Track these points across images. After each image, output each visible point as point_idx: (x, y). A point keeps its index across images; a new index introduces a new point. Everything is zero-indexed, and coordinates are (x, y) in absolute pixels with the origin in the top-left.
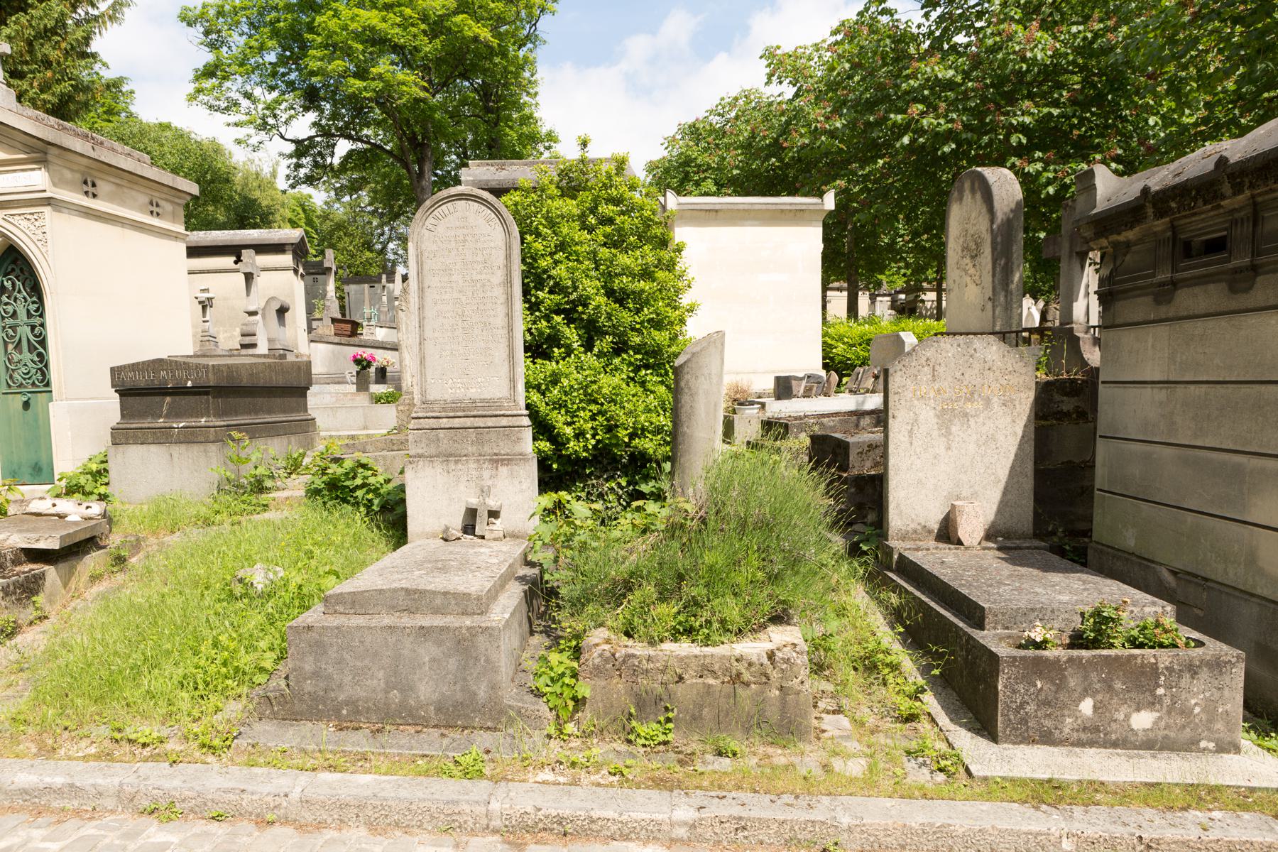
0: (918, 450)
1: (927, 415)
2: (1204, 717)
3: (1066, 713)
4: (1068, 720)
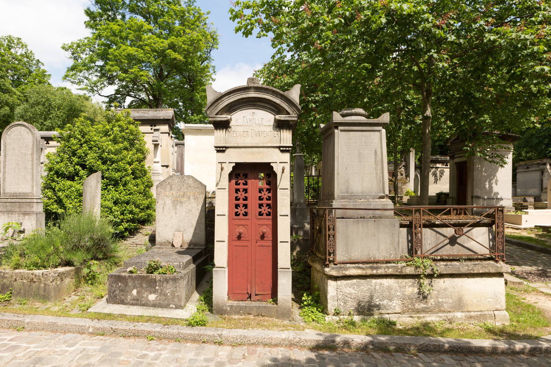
1: (169, 202)
4: (129, 296)
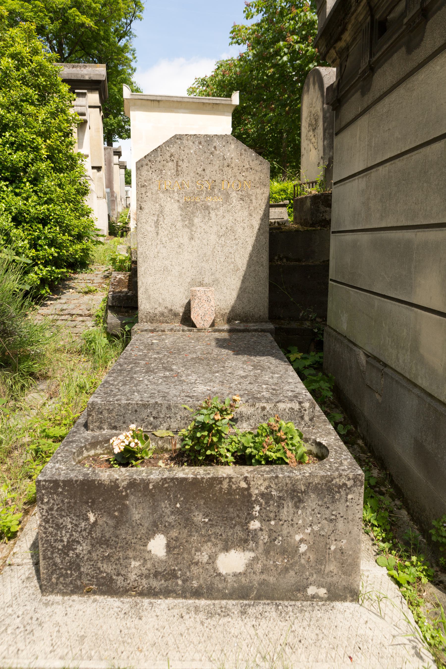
0: (164, 239)
1: (172, 207)
2: (312, 557)
3: (131, 554)
4: (134, 564)
